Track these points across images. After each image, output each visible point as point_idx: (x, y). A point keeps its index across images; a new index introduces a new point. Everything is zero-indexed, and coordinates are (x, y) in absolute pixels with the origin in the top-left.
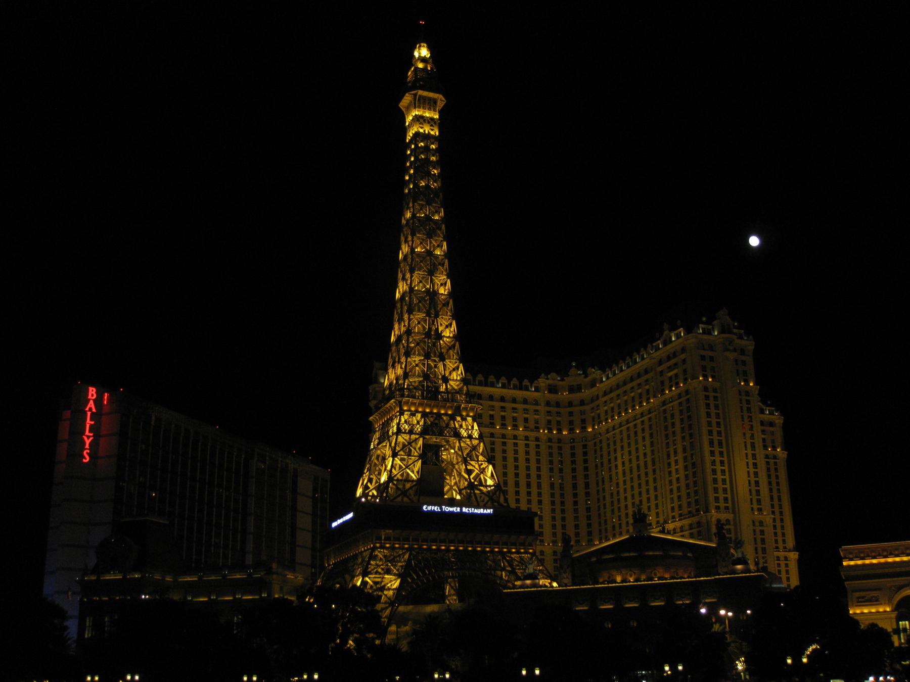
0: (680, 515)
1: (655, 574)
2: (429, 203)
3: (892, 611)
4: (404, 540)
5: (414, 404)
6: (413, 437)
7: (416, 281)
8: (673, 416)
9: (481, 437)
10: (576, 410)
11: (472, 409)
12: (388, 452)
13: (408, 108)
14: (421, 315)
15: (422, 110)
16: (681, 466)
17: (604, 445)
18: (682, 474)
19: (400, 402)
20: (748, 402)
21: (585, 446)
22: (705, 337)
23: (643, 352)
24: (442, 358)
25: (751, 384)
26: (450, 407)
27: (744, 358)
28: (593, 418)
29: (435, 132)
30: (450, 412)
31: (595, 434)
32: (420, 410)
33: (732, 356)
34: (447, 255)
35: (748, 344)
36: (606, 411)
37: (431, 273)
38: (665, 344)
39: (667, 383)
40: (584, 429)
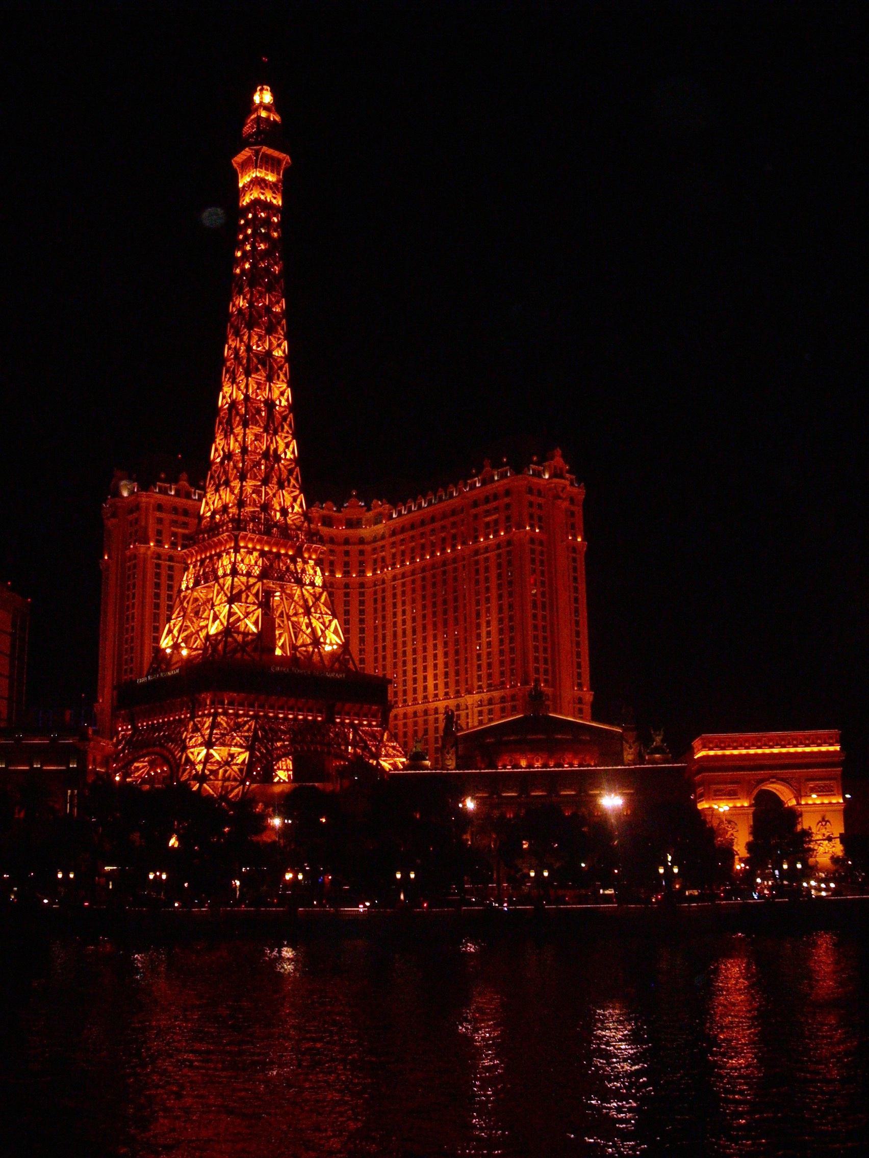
0: (489, 685)
1: (564, 760)
2: (270, 289)
3: (750, 806)
4: (259, 707)
5: (251, 540)
6: (252, 581)
8: (487, 569)
9: (324, 586)
11: (315, 551)
13: (246, 165)
14: (257, 430)
15: (264, 171)
16: (494, 628)
17: (389, 594)
18: (495, 638)
20: (574, 560)
22: (535, 480)
24: (281, 486)
25: (579, 540)
26: (292, 547)
27: (573, 508)
29: (278, 202)
30: (291, 553)
32: (258, 547)
34: (288, 358)
35: (578, 491)
36: (394, 555)
37: (270, 379)
38: (484, 483)
40: (362, 573)
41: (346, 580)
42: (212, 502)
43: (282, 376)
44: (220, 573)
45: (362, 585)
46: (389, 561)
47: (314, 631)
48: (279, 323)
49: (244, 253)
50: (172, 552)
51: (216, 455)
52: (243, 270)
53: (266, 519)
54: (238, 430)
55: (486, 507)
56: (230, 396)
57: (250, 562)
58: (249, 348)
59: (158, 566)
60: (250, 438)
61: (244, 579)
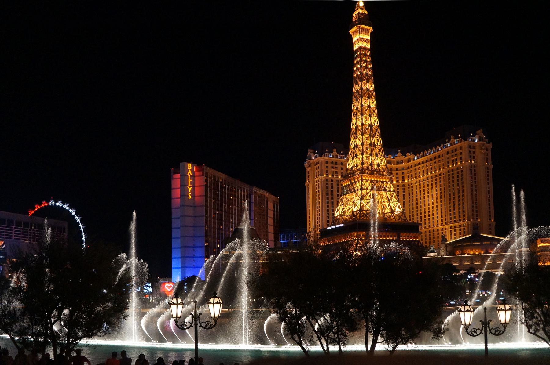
2: (368, 82)
6: (368, 191)
7: (364, 119)
10: (400, 172)
12: (357, 198)
19: (362, 176)
21: (404, 189)
22: (472, 142)
23: (438, 147)
28: (408, 176)
31: (410, 185)
33: (483, 151)
35: (490, 146)
37: (370, 116)
38: (451, 145)
39: (451, 162)
40: (403, 181)
41: (398, 184)
42: (352, 163)
43: (375, 114)
44: (356, 189)
45: (404, 185)
46: (414, 176)
47: (391, 208)
48: (372, 94)
49: (357, 68)
50: (333, 178)
51: (352, 146)
52: (357, 75)
53: (372, 169)
54: (360, 136)
55: (453, 154)
56: (356, 124)
57: (367, 185)
58: (362, 105)
59: (327, 184)
60: (364, 138)
61: (365, 191)
